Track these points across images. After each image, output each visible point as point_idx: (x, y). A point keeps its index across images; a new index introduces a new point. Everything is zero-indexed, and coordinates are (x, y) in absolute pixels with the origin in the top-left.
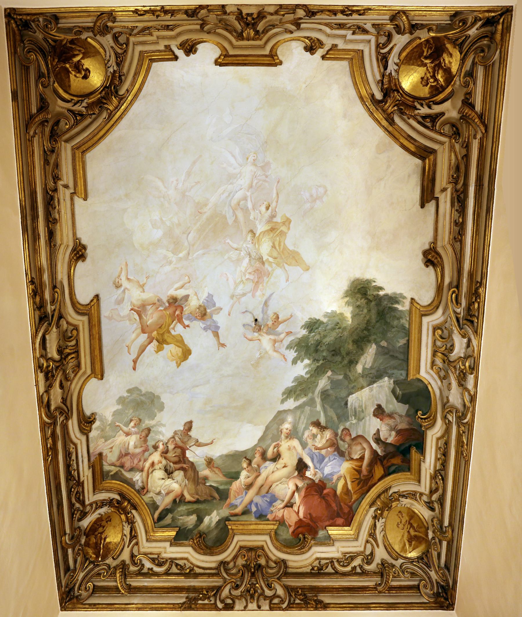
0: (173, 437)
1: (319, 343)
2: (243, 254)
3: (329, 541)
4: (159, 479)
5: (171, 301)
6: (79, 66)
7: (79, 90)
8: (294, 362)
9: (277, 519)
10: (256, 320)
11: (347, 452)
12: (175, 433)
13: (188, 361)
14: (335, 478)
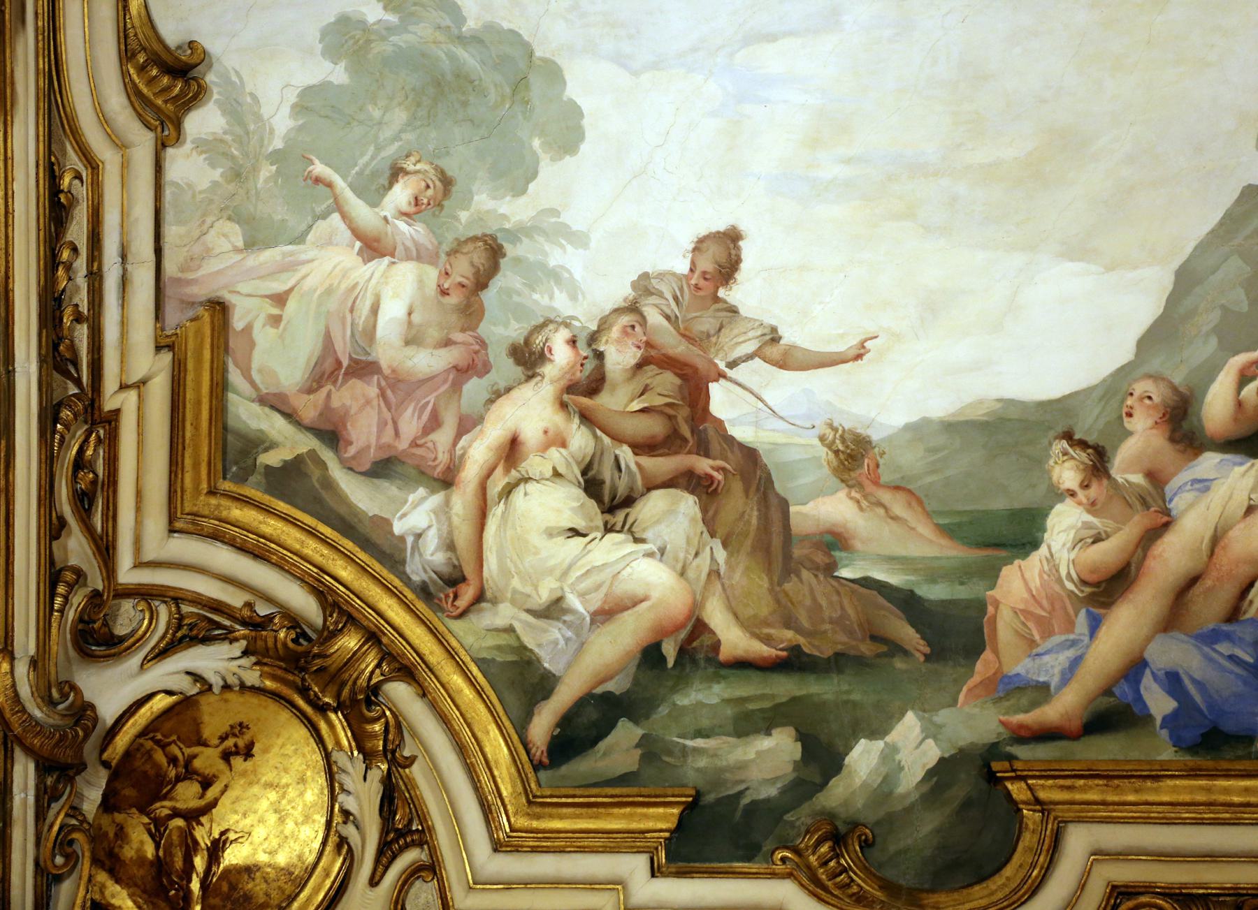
0: (633, 308)
4: (550, 533)
12: (644, 285)
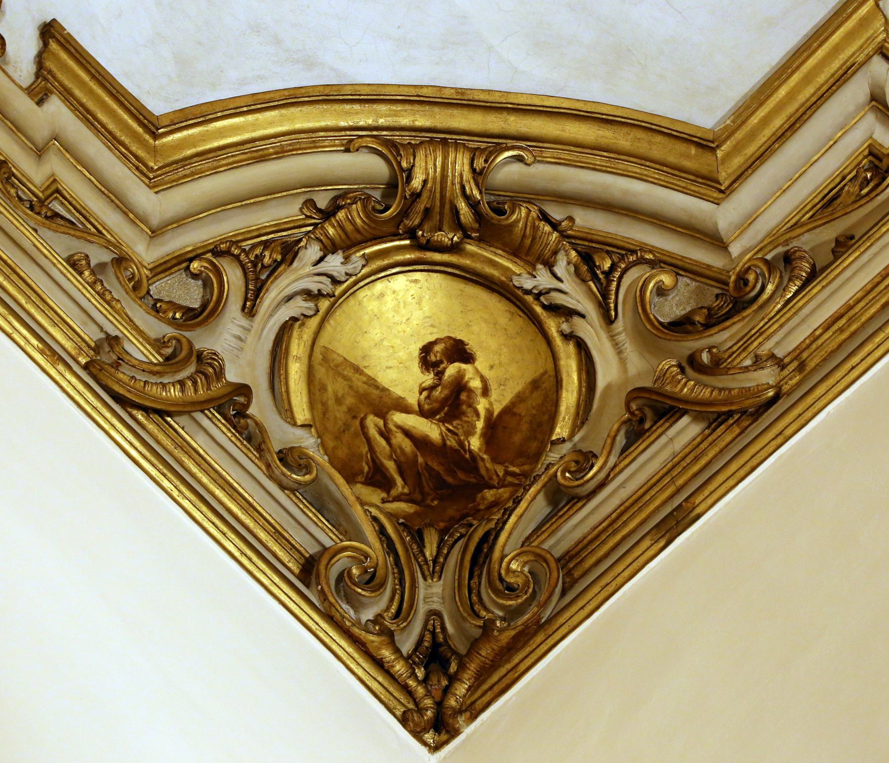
6: (444, 402)
7: (517, 341)
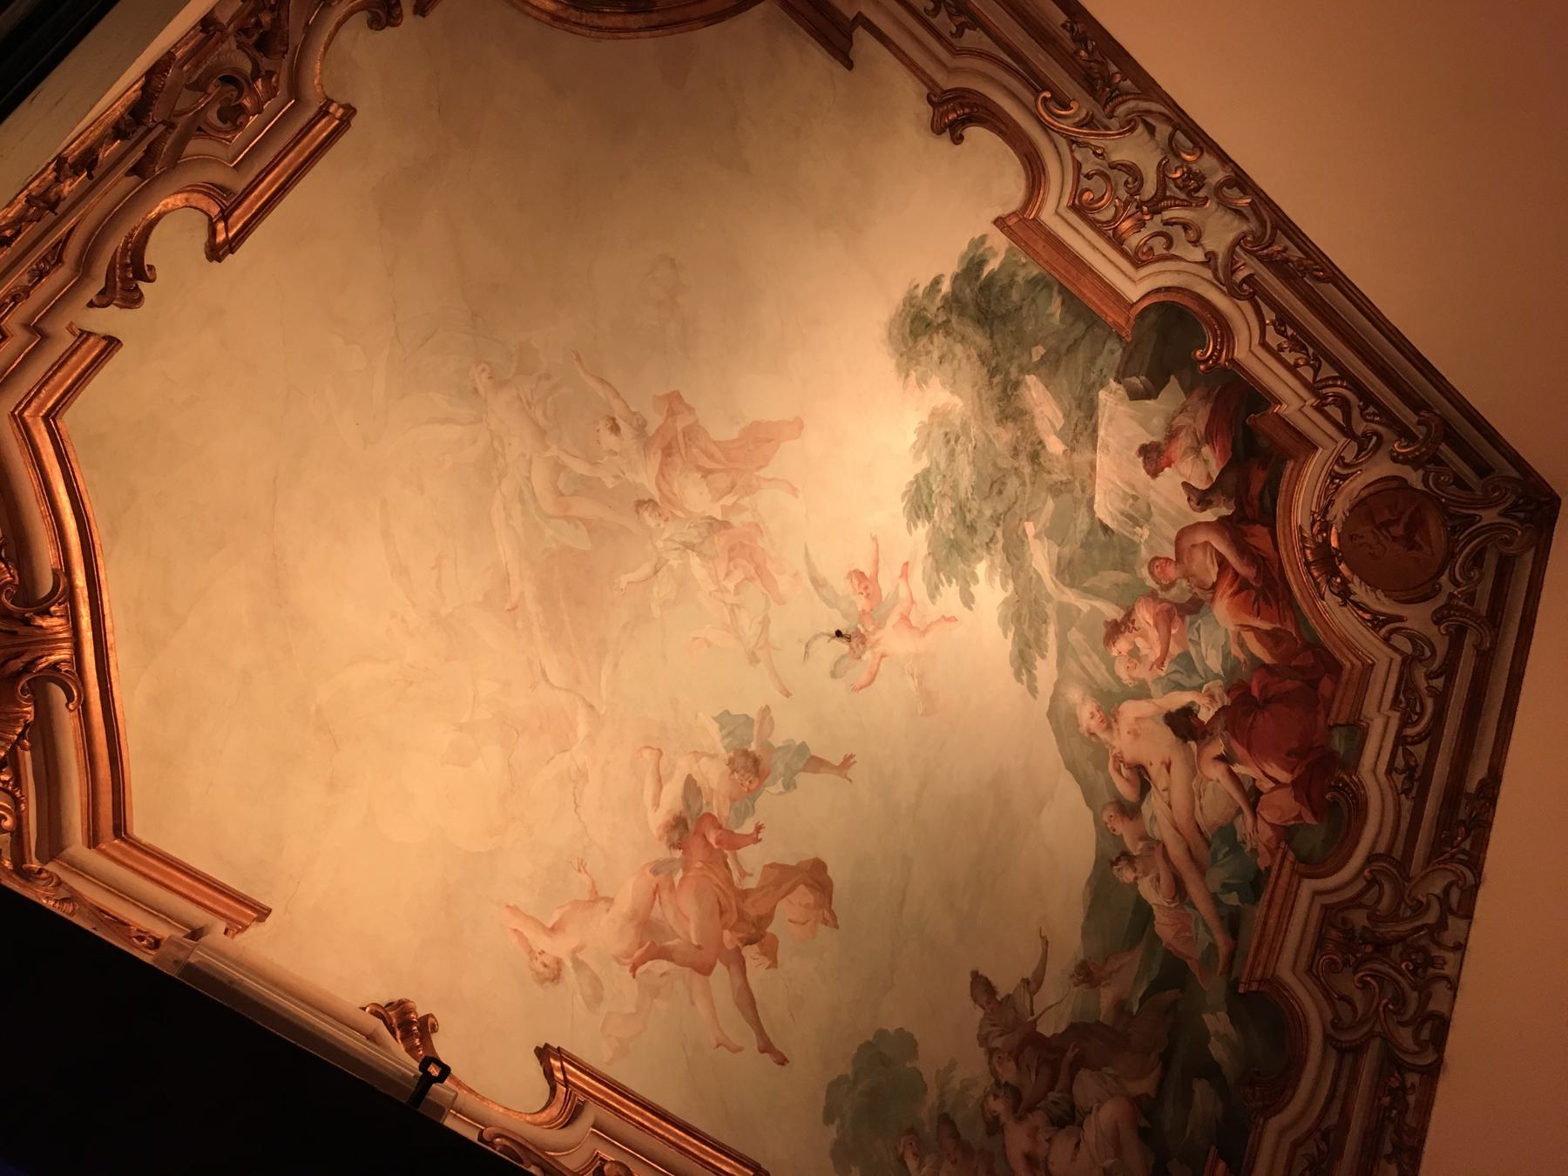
0: (991, 1052)
1: (960, 510)
2: (674, 563)
3: (1357, 731)
4: (1073, 1160)
5: (676, 837)
8: (968, 600)
9: (1273, 845)
10: (839, 634)
11: (1197, 590)
12: (983, 1040)
13: (837, 886)
14: (1235, 650)
